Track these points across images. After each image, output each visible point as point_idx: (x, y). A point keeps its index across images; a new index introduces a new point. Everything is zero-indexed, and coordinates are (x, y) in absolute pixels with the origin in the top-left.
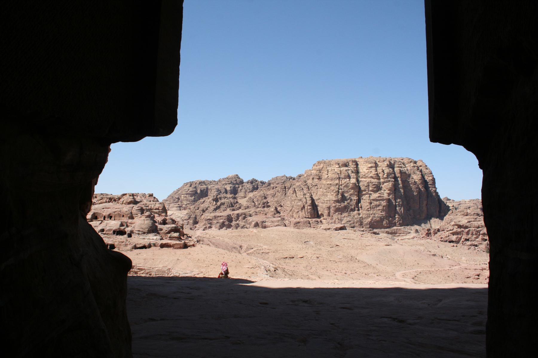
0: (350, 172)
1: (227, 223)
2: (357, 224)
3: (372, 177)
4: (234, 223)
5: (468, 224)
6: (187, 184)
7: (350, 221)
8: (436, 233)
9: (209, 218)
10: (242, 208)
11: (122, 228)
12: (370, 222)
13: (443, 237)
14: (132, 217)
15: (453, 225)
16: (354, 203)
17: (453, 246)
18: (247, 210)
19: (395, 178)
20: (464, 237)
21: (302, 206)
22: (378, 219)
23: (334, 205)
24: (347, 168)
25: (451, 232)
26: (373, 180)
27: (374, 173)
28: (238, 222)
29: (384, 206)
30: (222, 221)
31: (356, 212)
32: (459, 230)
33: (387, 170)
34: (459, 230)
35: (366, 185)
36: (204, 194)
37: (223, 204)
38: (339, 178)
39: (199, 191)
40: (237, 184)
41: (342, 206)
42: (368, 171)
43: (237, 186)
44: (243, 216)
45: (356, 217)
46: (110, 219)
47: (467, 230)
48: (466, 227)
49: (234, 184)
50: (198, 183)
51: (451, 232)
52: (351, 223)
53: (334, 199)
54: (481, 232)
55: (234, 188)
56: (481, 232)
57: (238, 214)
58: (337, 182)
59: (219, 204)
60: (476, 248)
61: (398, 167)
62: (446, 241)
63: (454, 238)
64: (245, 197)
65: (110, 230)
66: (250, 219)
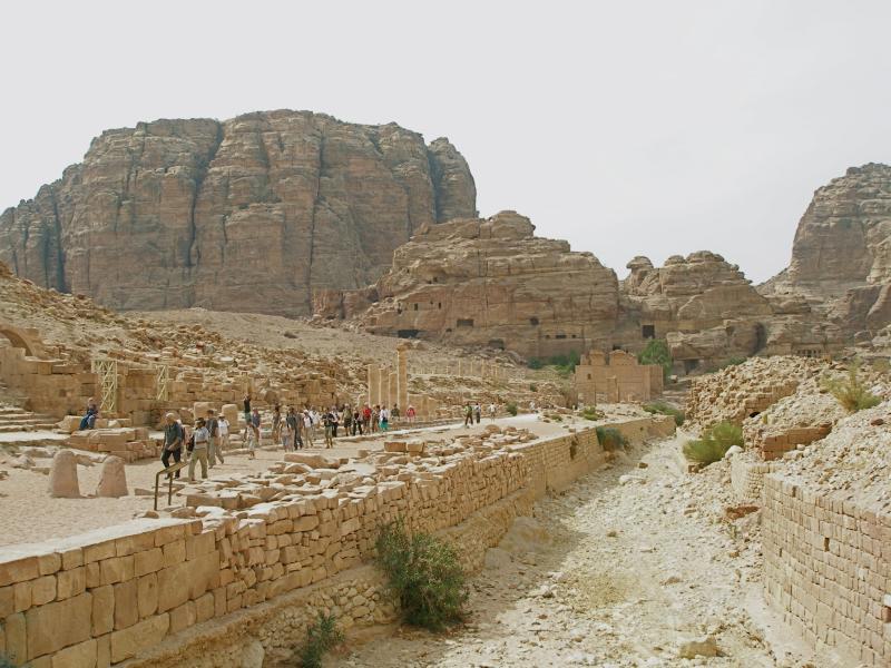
20: (455, 314)
47: (466, 284)
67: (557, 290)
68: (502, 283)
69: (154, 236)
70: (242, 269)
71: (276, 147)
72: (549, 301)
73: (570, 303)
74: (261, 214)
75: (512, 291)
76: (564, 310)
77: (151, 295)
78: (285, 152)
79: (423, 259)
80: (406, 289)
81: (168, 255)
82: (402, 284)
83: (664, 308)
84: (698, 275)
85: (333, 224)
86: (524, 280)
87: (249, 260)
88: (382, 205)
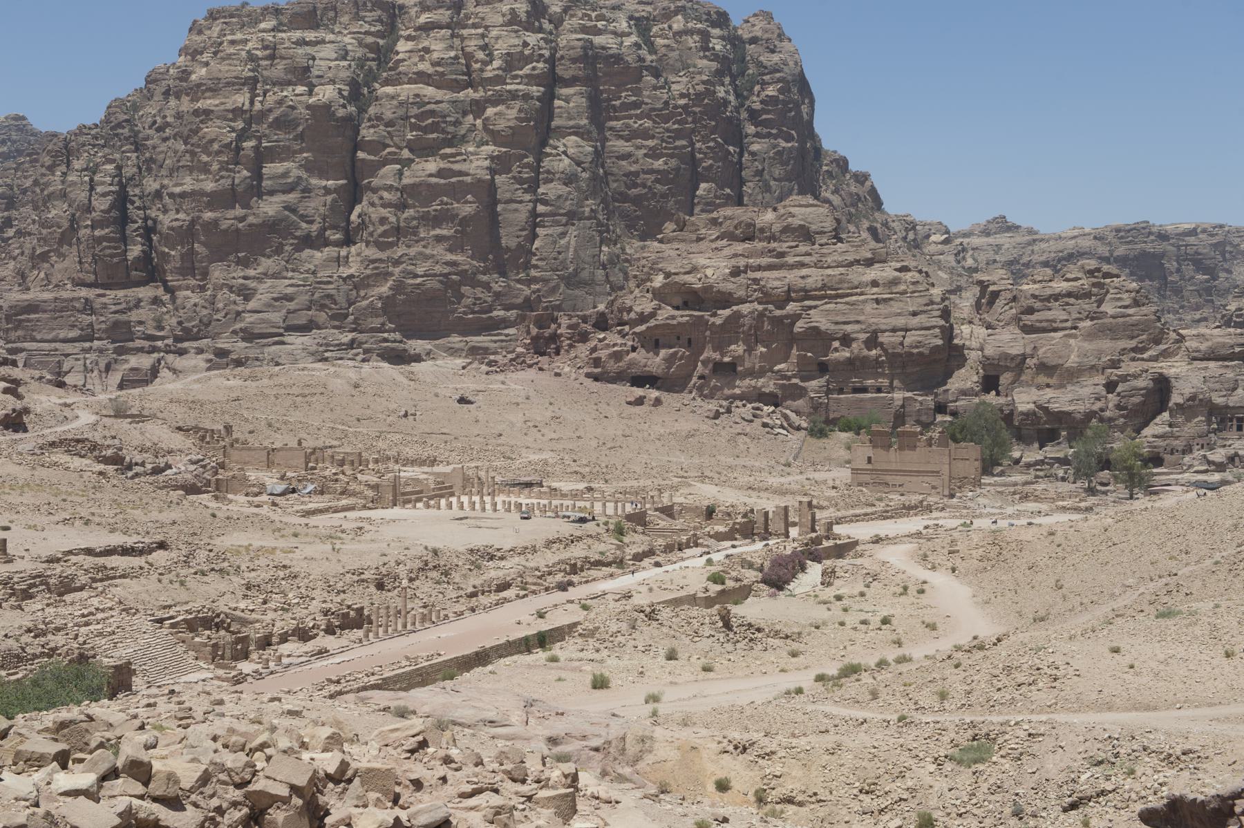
0: (327, 51)
2: (322, 317)
3: (422, 77)
5: (735, 287)
7: (289, 298)
8: (584, 338)
12: (388, 302)
13: (603, 354)
15: (658, 294)
16: (317, 205)
17: (640, 401)
19: (551, 81)
21: (66, 224)
22: (433, 284)
23: (208, 215)
24: (310, 35)
25: (643, 327)
26: (429, 91)
27: (435, 56)
29: (464, 222)
31: (329, 251)
32: (683, 316)
33: (505, 42)
34: (683, 316)
35: (388, 115)
38: (252, 83)
41: (251, 219)
42: (410, 45)
45: (323, 275)
48: (726, 300)
51: (643, 327)
52: (292, 305)
53: (209, 186)
54: (800, 326)
56: (800, 326)
58: (241, 99)
60: (768, 409)
61: (584, 29)
62: (613, 380)
63: (655, 362)
67: (858, 322)
68: (778, 313)
69: (292, 197)
70: (428, 251)
71: (481, 55)
72: (846, 340)
73: (872, 342)
74: (456, 167)
75: (793, 324)
76: (865, 352)
77: (290, 290)
78: (496, 64)
79: (668, 275)
80: (643, 318)
81: (315, 227)
82: (638, 309)
83: (1014, 351)
84: (1072, 300)
85: (569, 179)
86: (810, 308)
87: (439, 239)
88: (650, 143)
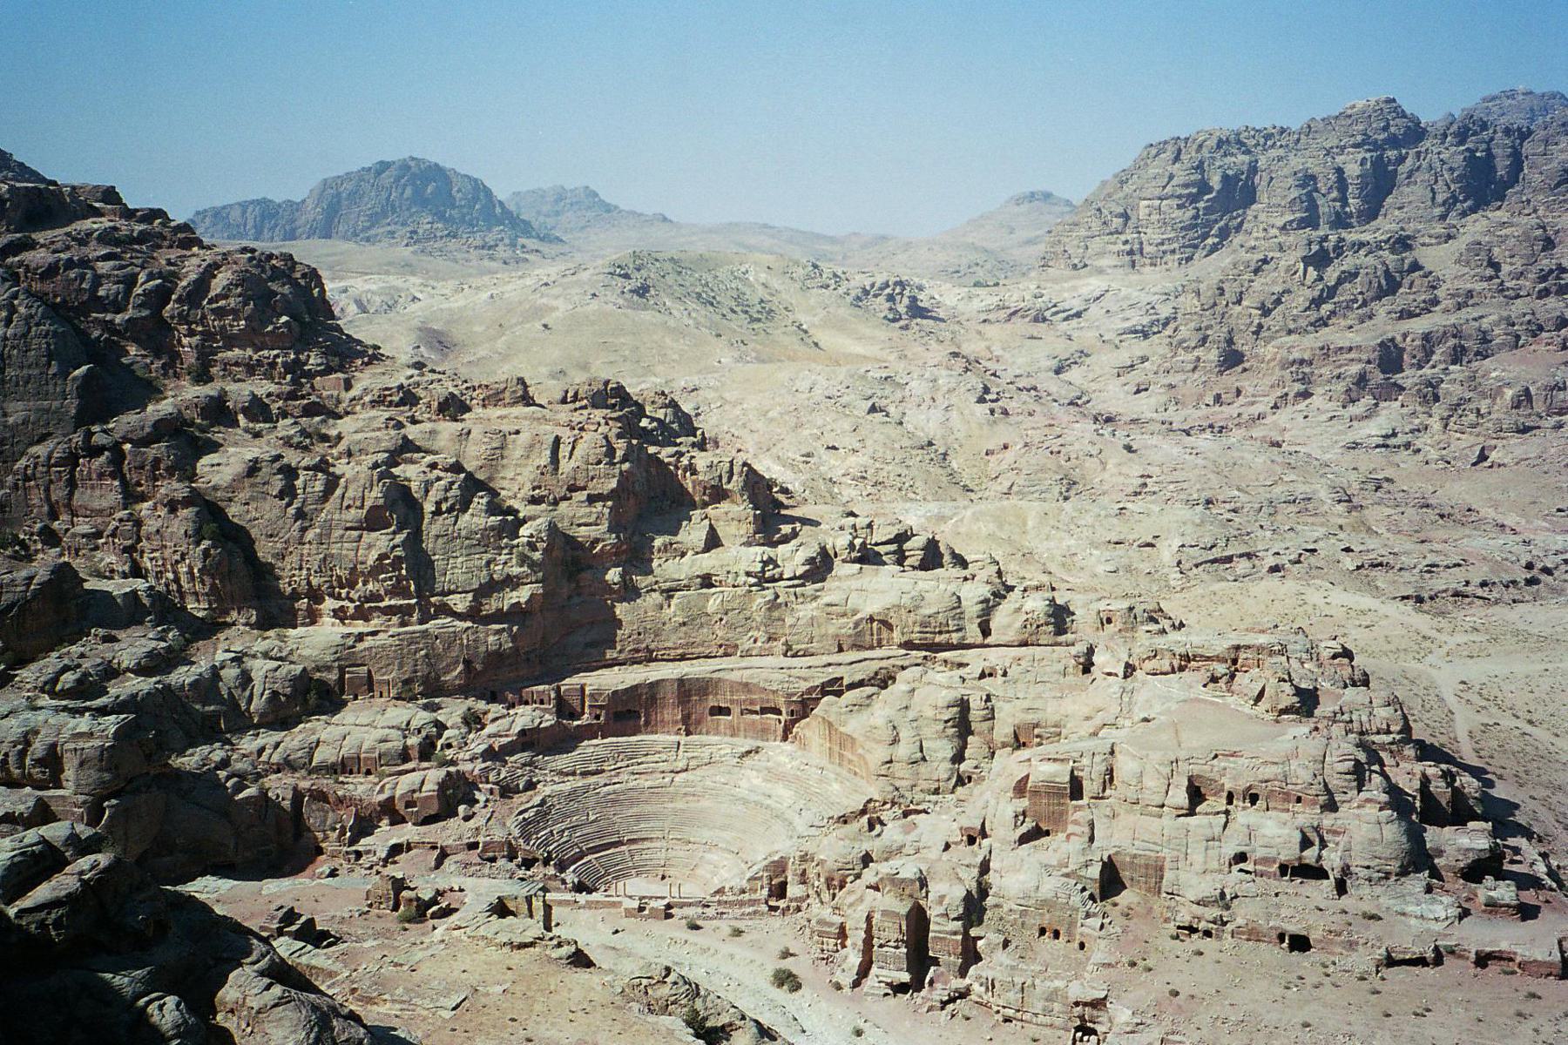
1: (1377, 377)
4: (1409, 377)
6: (1161, 147)
9: (1296, 355)
10: (1447, 303)
11: (1310, 855)
14: (1331, 806)
18: (1465, 314)
28: (1427, 371)
30: (1355, 369)
36: (1239, 193)
37: (1352, 276)
39: (1215, 181)
40: (1394, 142)
43: (1391, 154)
44: (1452, 342)
46: (1253, 803)
49: (1376, 146)
50: (1213, 142)
55: (1379, 163)
57: (1427, 337)
59: (1332, 274)
64: (1449, 237)
65: (1266, 861)
66: (1496, 369)
